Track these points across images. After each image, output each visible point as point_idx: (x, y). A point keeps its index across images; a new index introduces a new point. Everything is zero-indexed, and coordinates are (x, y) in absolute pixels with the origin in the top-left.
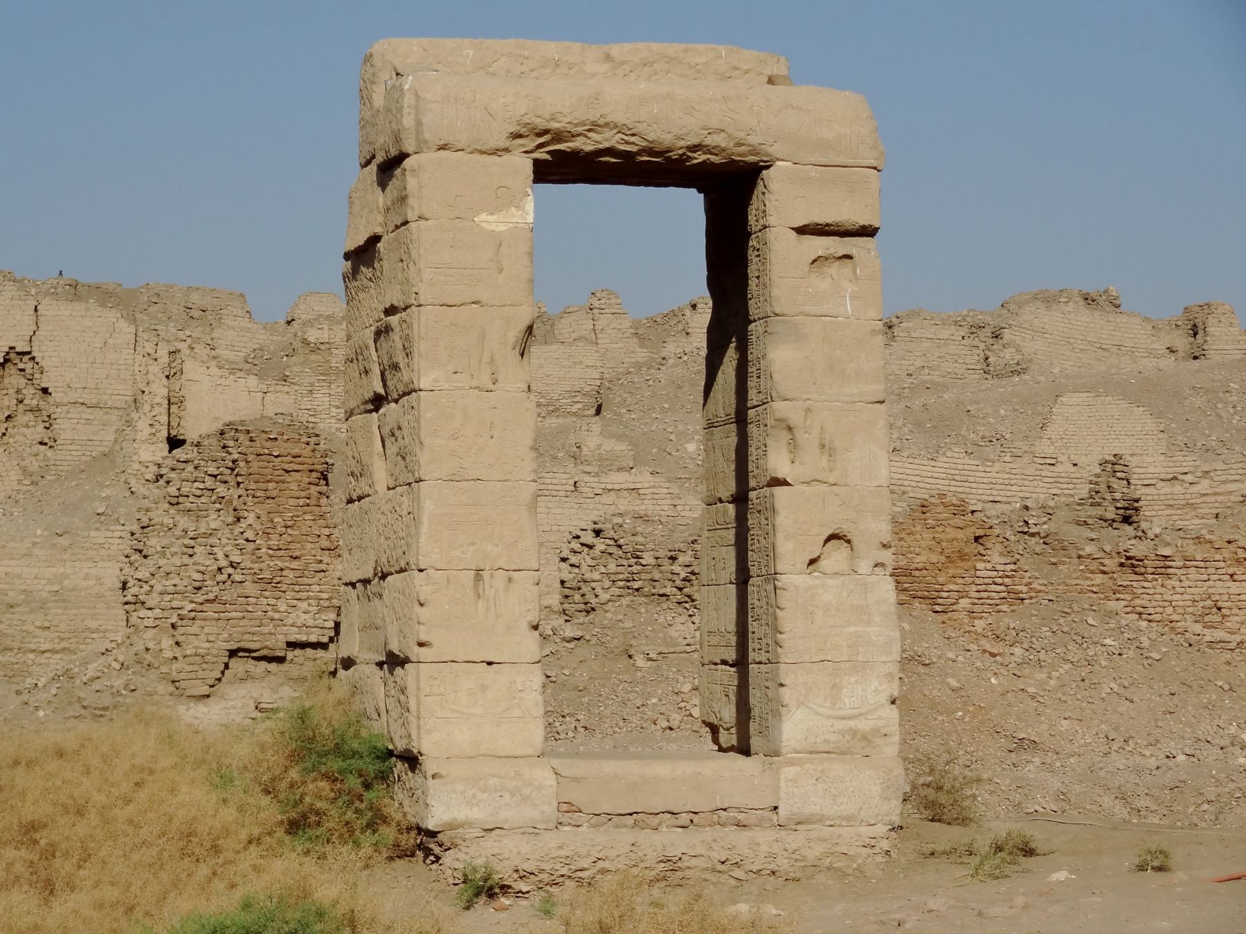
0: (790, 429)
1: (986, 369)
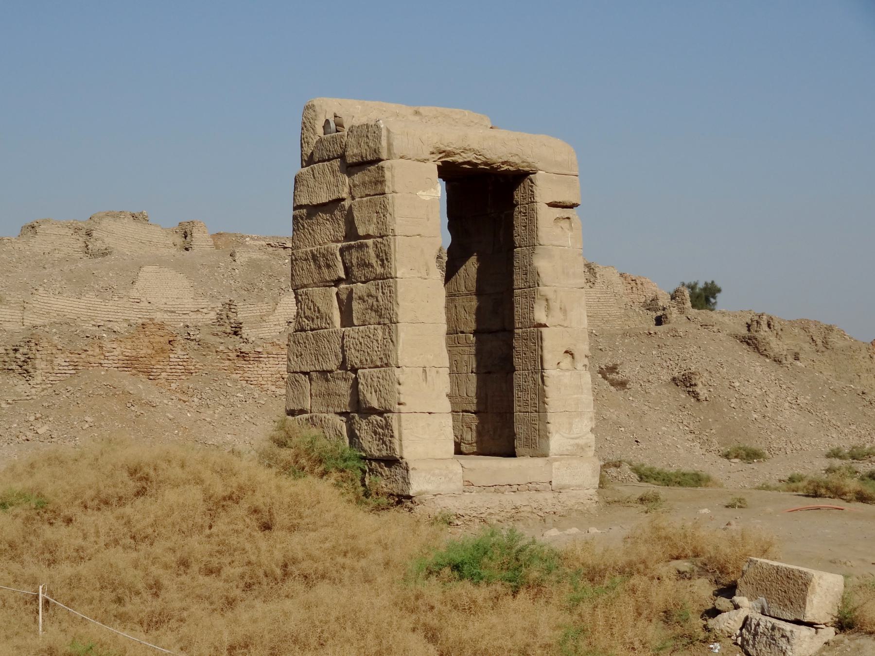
0: (547, 300)
1: (87, 251)
